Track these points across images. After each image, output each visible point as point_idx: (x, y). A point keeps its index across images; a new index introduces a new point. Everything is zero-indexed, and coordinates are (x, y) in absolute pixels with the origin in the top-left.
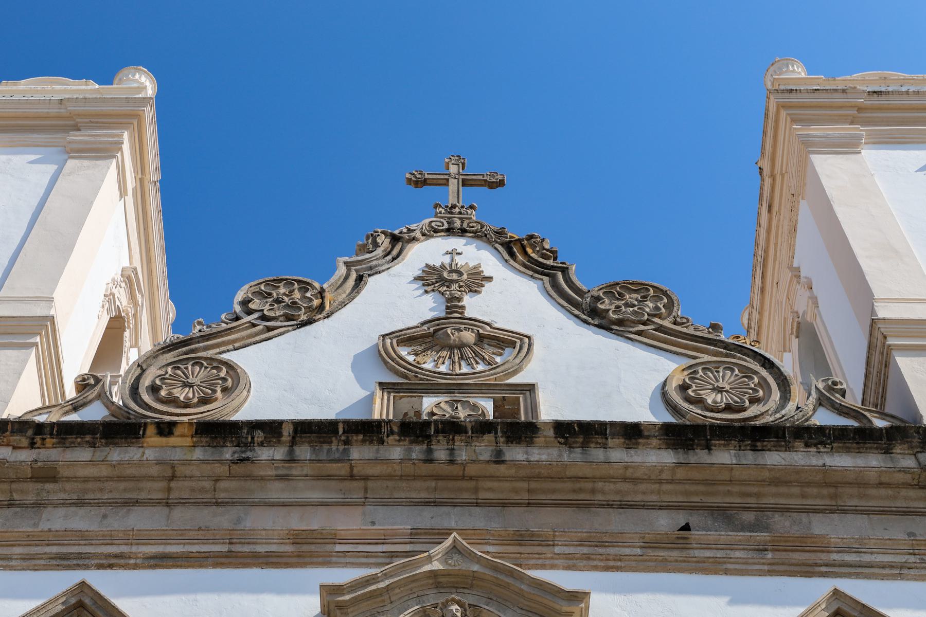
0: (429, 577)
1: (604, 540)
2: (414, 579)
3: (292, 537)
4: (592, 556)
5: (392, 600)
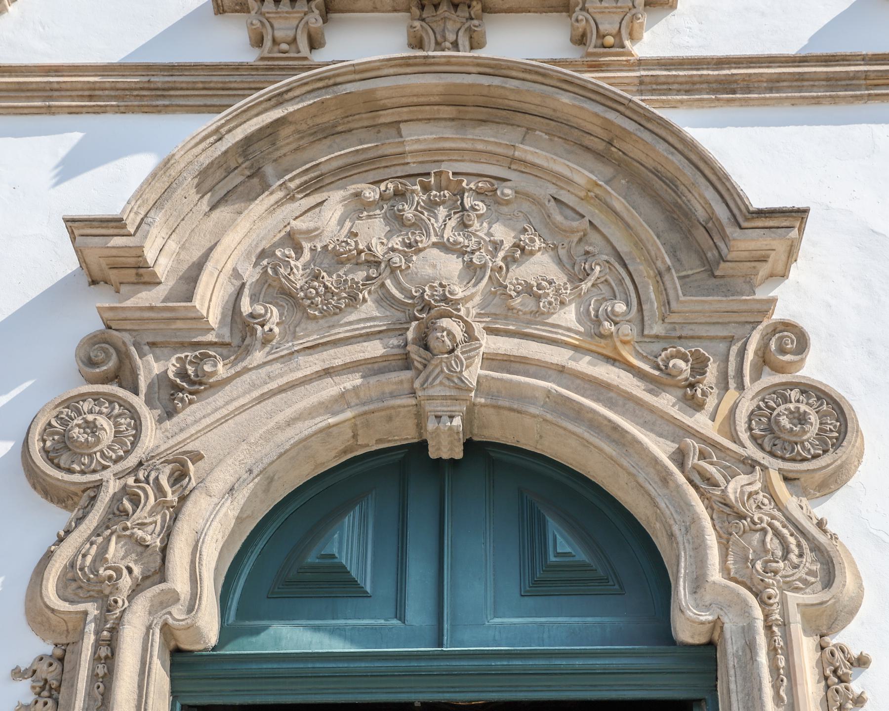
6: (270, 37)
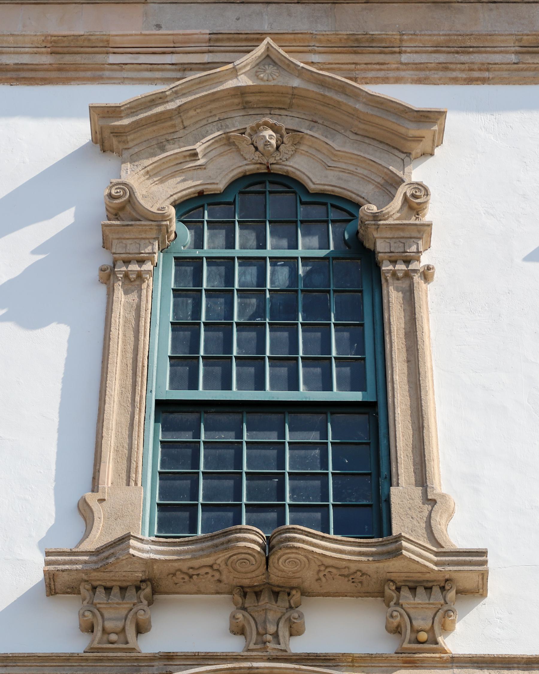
0: (234, 96)
1: (468, 44)
2: (214, 98)
3: (49, 45)
4: (451, 66)
5: (186, 124)
6: (100, 628)
